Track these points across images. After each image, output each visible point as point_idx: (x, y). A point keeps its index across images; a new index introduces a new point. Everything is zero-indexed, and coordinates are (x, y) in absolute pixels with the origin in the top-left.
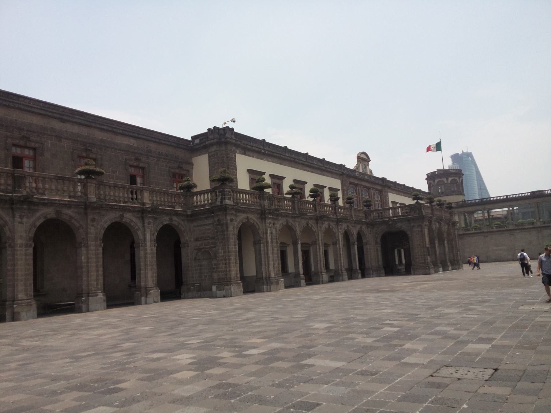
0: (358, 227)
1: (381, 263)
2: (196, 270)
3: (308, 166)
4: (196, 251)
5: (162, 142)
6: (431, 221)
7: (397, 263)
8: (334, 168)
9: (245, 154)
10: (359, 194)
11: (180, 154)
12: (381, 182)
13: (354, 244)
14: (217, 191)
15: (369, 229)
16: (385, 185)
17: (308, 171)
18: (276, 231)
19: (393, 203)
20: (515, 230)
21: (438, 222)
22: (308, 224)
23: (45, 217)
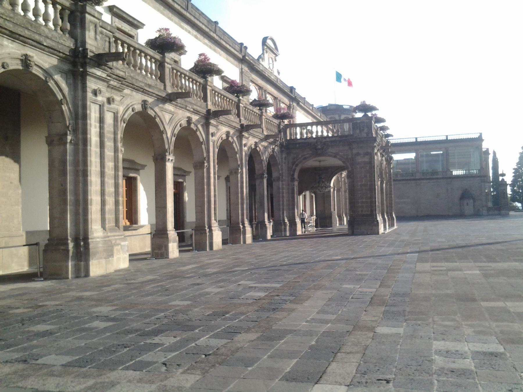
13: (262, 178)
18: (115, 119)
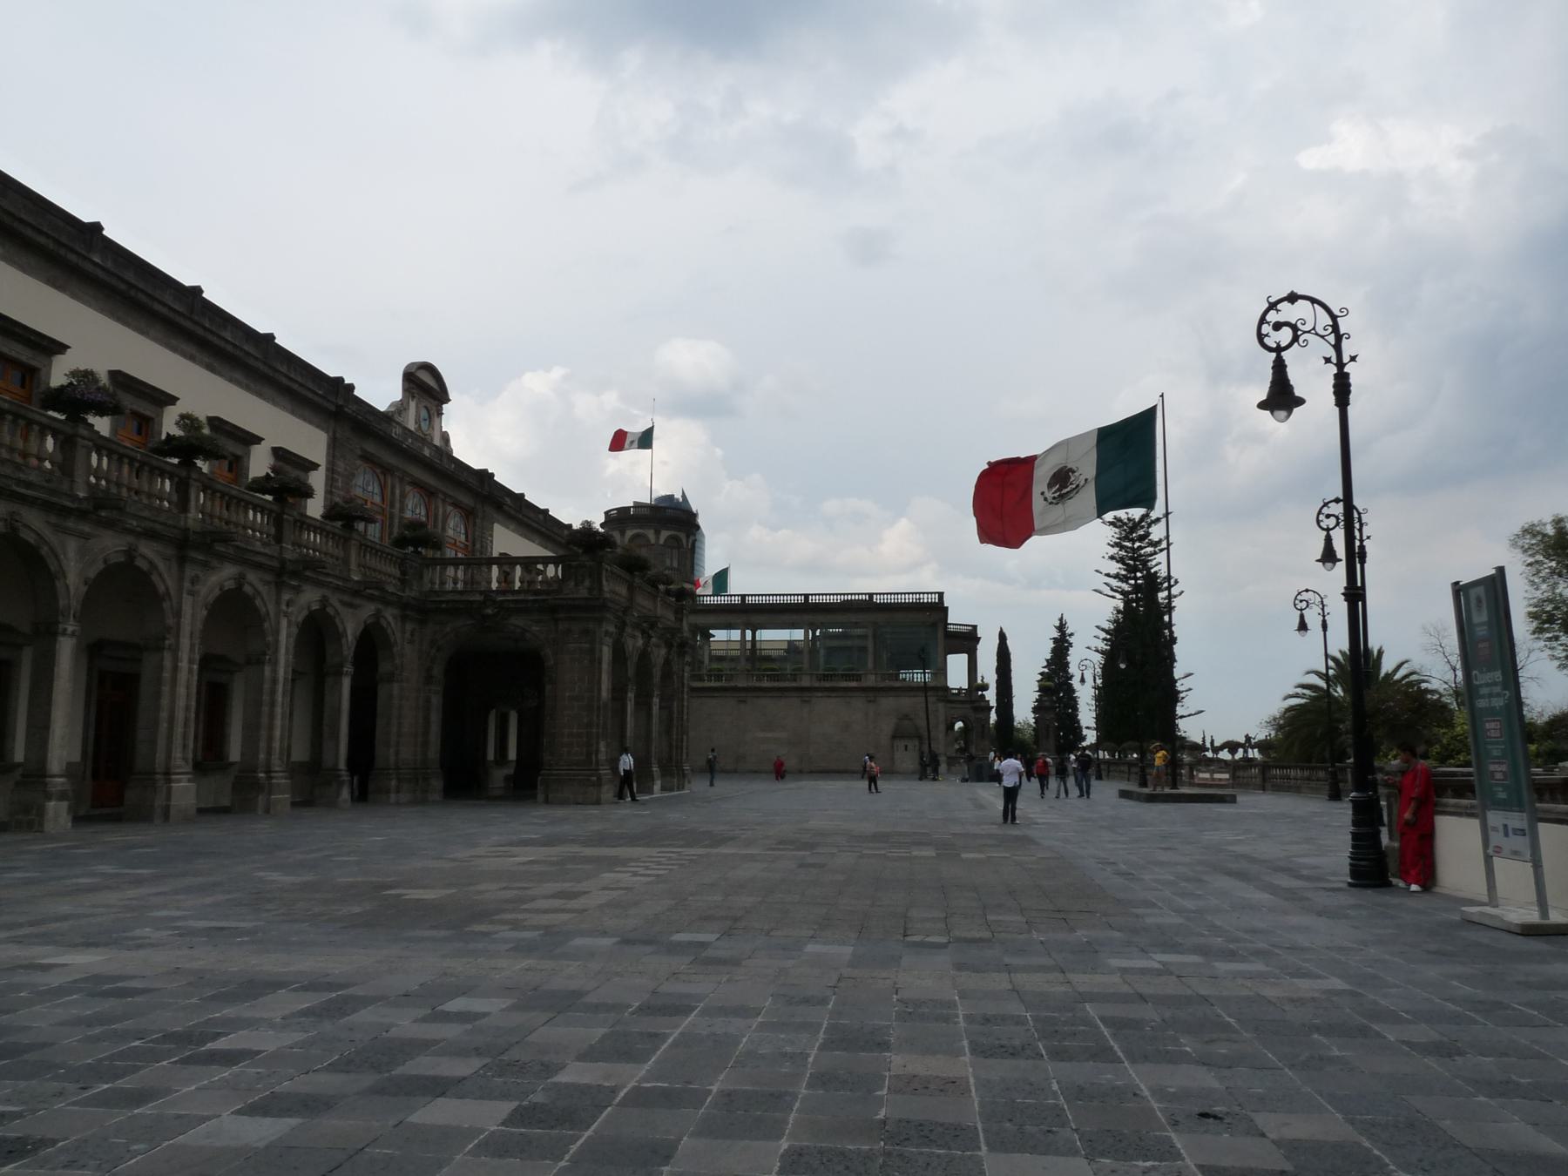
0: (368, 610)
1: (434, 752)
3: (190, 337)
6: (624, 624)
7: (491, 756)
8: (310, 385)
10: (392, 506)
13: (339, 674)
15: (409, 627)
16: (485, 496)
17: (192, 358)
21: (644, 632)
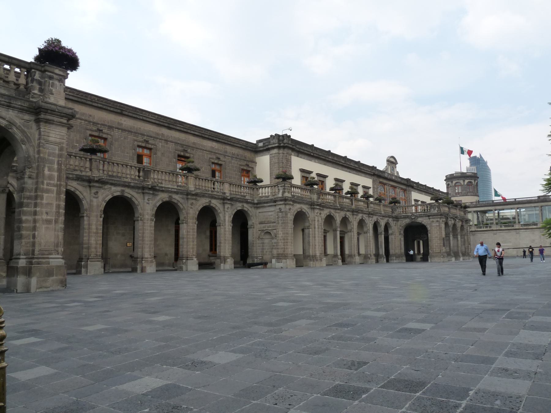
0: (386, 219)
1: (403, 251)
2: (259, 246)
4: (260, 232)
5: (235, 145)
9: (298, 156)
11: (248, 155)
12: (406, 182)
14: (280, 185)
18: (322, 219)
19: (416, 200)
20: (521, 229)
22: (345, 215)
23: (162, 200)
